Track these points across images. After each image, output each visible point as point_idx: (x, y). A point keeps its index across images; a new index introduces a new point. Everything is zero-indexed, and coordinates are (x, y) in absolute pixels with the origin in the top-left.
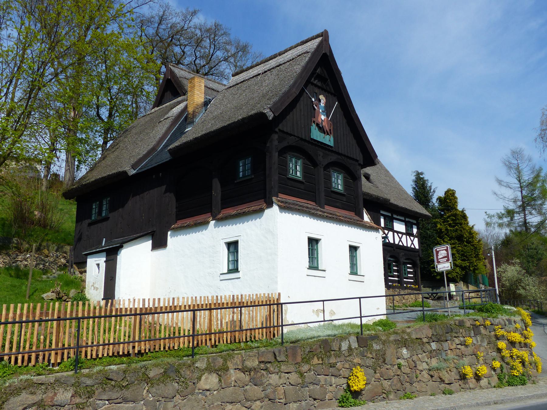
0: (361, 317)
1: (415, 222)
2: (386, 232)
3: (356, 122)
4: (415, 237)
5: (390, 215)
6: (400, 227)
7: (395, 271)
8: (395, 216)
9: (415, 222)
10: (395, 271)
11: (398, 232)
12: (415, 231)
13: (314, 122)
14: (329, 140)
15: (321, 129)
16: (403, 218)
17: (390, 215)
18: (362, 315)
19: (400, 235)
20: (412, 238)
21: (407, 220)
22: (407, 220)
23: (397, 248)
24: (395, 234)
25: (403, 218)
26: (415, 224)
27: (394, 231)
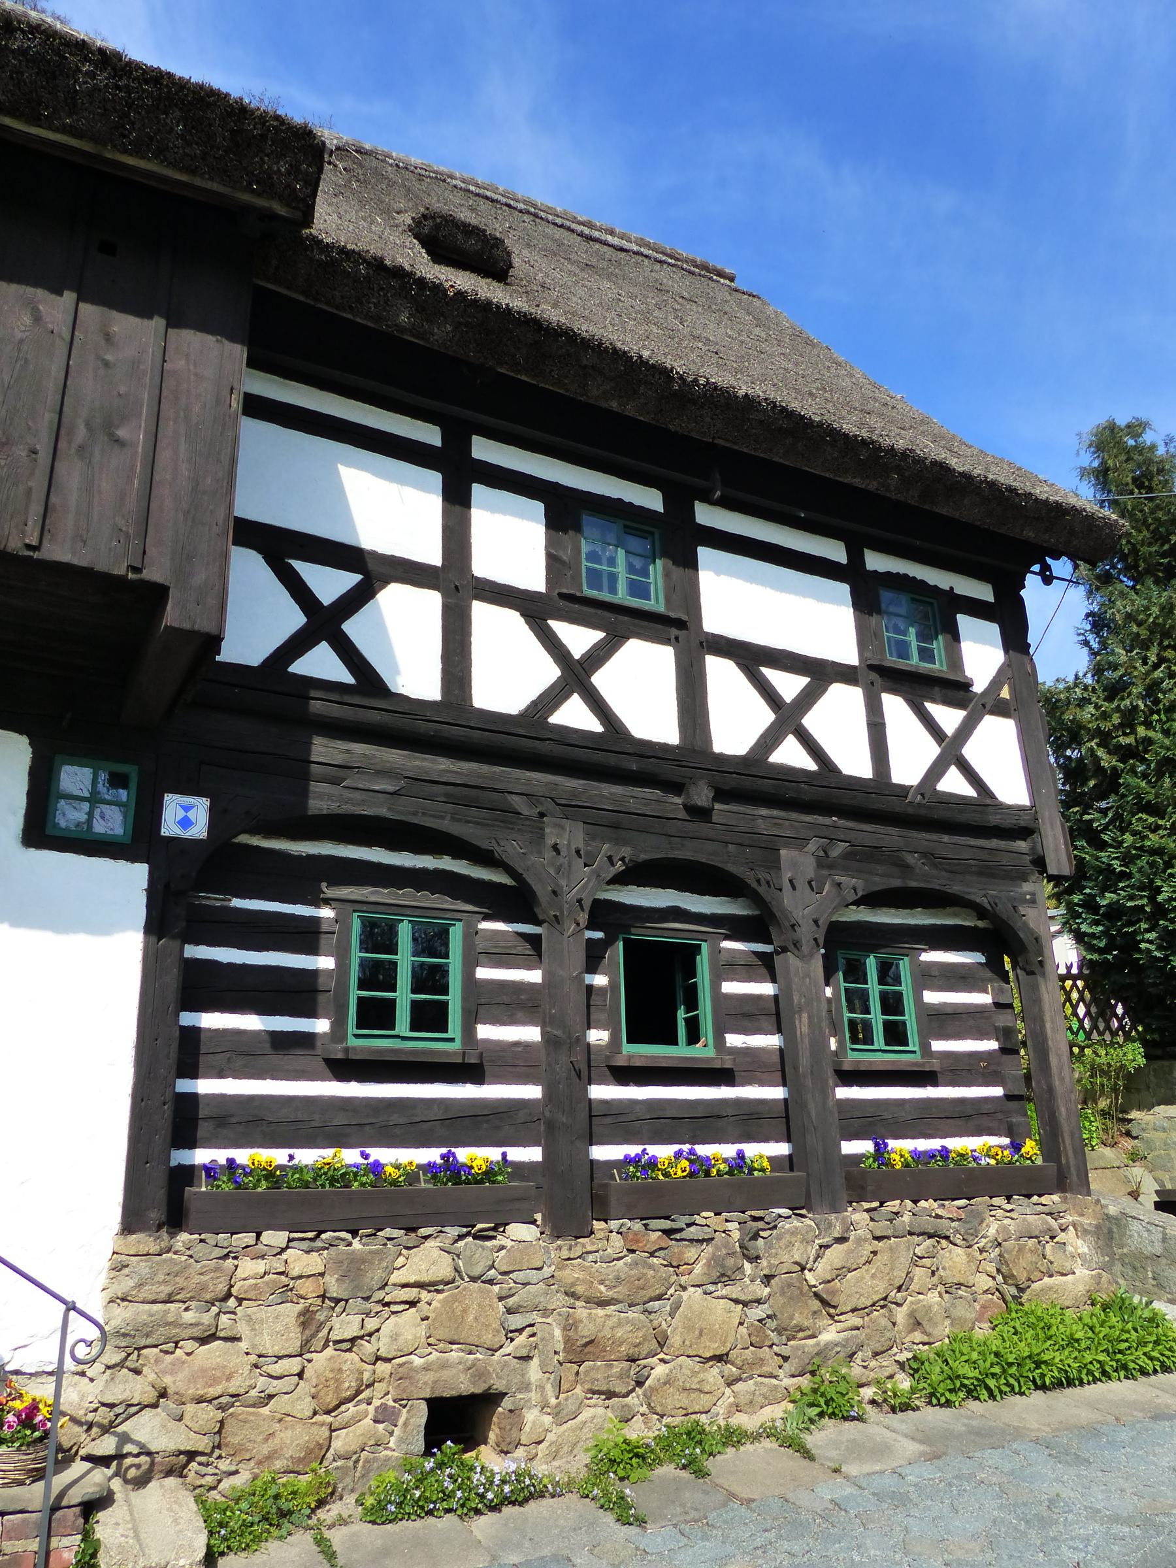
1: (983, 592)
2: (579, 639)
4: (977, 706)
5: (651, 499)
7: (746, 1014)
8: (707, 515)
9: (983, 592)
10: (746, 1014)
11: (752, 659)
16: (836, 552)
17: (651, 499)
19: (789, 685)
20: (949, 718)
21: (876, 562)
22: (876, 562)
23: (722, 795)
24: (721, 674)
25: (836, 552)
26: (977, 609)
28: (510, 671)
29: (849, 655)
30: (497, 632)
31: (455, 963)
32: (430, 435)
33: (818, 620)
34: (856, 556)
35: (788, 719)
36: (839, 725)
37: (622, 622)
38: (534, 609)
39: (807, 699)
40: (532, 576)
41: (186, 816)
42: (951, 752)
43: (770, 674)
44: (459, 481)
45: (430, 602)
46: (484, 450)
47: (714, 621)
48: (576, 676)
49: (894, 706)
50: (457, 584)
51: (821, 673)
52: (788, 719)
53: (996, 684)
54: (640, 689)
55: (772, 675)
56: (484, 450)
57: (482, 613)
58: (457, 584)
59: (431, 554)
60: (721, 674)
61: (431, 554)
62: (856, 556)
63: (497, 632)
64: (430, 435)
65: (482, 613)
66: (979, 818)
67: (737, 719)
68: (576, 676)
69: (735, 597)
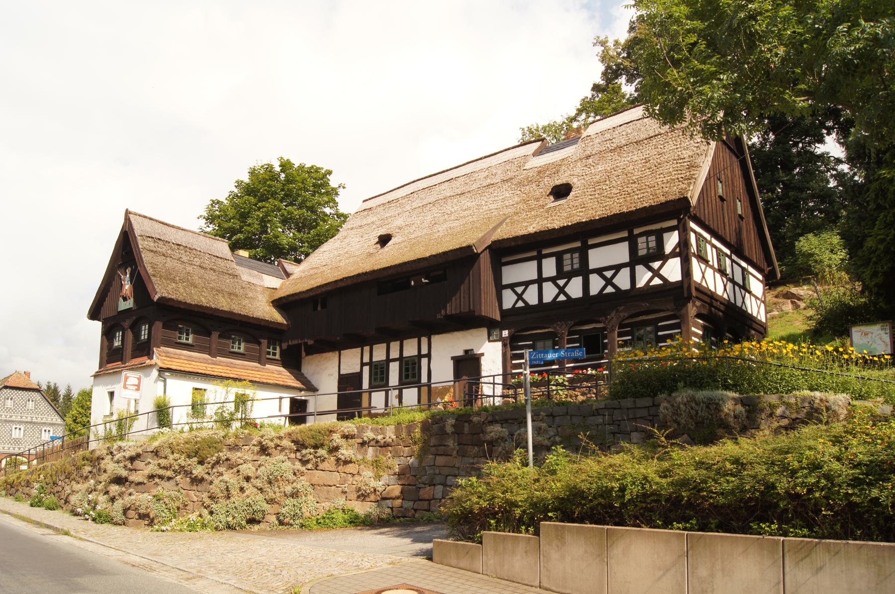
2: (561, 282)
4: (664, 258)
6: (608, 254)
11: (600, 271)
20: (656, 265)
27: (584, 271)
28: (550, 292)
33: (619, 253)
34: (631, 232)
38: (553, 280)
41: (505, 333)
42: (656, 273)
48: (562, 290)
49: (640, 269)
51: (617, 268)
53: (675, 248)
54: (575, 289)
67: (596, 284)
68: (562, 290)
69: (598, 258)
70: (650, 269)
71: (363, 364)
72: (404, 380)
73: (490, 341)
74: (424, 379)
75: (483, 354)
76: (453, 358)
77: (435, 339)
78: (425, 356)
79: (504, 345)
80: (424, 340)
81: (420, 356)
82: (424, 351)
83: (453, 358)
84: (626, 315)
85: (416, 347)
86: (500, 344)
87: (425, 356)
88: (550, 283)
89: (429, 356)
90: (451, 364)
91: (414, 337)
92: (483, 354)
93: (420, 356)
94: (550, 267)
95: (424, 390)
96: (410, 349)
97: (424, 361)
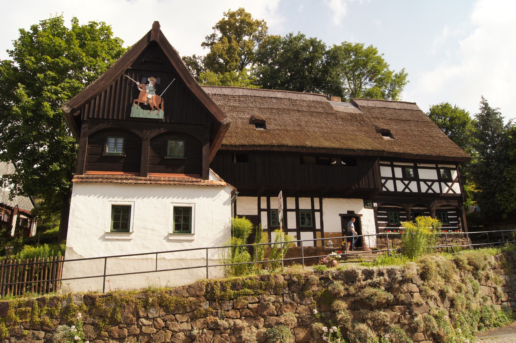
0: (104, 276)
1: (454, 167)
2: (406, 182)
3: (193, 91)
4: (453, 182)
5: (412, 165)
6: (427, 174)
8: (418, 165)
9: (454, 167)
11: (425, 181)
12: (455, 175)
13: (136, 103)
14: (159, 114)
15: (146, 107)
16: (434, 166)
17: (412, 165)
18: (106, 274)
19: (429, 183)
20: (450, 184)
21: (439, 166)
22: (439, 166)
24: (422, 184)
25: (434, 166)
28: (400, 187)
29: (436, 177)
30: (398, 183)
31: (397, 216)
32: (389, 163)
33: (432, 174)
34: (437, 166)
35: (430, 187)
36: (436, 187)
37: (411, 180)
38: (402, 180)
39: (432, 185)
40: (401, 176)
41: (375, 205)
42: (450, 188)
43: (427, 182)
44: (393, 167)
45: (392, 181)
46: (395, 164)
47: (421, 177)
48: (407, 186)
49: (443, 184)
50: (394, 179)
51: (433, 181)
52: (430, 187)
53: (456, 179)
54: (413, 187)
55: (427, 182)
56: (395, 164)
57: (397, 181)
58: (394, 179)
59: (391, 176)
60: (422, 184)
61: (391, 176)
62: (437, 166)
63: (398, 183)
64: (389, 163)
65: (397, 181)
66: (454, 197)
67: (424, 188)
68: (407, 186)
69: (423, 174)
70: (447, 185)
71: (260, 210)
72: (301, 226)
73: (365, 208)
74: (318, 226)
75: (362, 215)
76: (340, 215)
77: (326, 201)
78: (317, 211)
79: (375, 212)
80: (317, 201)
81: (313, 210)
82: (317, 207)
83: (340, 215)
84: (439, 205)
85: (310, 203)
86: (372, 211)
87: (317, 211)
88: (400, 181)
89: (321, 211)
90: (339, 219)
91: (308, 197)
92: (362, 215)
93: (313, 210)
94: (398, 172)
95: (318, 234)
96: (305, 204)
97: (317, 215)
